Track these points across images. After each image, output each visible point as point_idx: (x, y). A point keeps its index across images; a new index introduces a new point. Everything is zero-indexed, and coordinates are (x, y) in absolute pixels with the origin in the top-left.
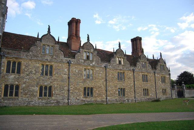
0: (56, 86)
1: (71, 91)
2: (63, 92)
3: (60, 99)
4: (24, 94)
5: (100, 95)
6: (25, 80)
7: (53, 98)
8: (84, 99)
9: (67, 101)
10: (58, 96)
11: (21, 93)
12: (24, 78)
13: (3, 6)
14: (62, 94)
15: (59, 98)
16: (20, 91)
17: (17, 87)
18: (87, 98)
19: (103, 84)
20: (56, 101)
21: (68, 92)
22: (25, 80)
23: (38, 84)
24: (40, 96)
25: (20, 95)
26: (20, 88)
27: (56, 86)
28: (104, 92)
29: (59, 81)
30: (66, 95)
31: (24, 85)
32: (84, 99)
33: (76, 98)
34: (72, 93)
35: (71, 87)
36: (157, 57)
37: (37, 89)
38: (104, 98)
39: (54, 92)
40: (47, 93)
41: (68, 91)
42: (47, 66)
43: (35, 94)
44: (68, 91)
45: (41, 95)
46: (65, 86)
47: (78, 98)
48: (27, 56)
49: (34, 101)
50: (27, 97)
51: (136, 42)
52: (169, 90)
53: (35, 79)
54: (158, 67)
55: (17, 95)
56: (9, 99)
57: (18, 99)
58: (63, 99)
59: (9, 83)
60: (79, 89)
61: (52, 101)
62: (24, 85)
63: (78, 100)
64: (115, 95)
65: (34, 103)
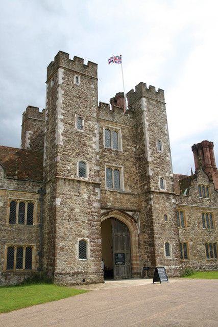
4: (193, 255)
13: (167, 137)
16: (189, 251)
23: (203, 241)
25: (190, 256)
31: (191, 243)
37: (203, 247)
42: (207, 214)
48: (188, 201)
62: (191, 243)
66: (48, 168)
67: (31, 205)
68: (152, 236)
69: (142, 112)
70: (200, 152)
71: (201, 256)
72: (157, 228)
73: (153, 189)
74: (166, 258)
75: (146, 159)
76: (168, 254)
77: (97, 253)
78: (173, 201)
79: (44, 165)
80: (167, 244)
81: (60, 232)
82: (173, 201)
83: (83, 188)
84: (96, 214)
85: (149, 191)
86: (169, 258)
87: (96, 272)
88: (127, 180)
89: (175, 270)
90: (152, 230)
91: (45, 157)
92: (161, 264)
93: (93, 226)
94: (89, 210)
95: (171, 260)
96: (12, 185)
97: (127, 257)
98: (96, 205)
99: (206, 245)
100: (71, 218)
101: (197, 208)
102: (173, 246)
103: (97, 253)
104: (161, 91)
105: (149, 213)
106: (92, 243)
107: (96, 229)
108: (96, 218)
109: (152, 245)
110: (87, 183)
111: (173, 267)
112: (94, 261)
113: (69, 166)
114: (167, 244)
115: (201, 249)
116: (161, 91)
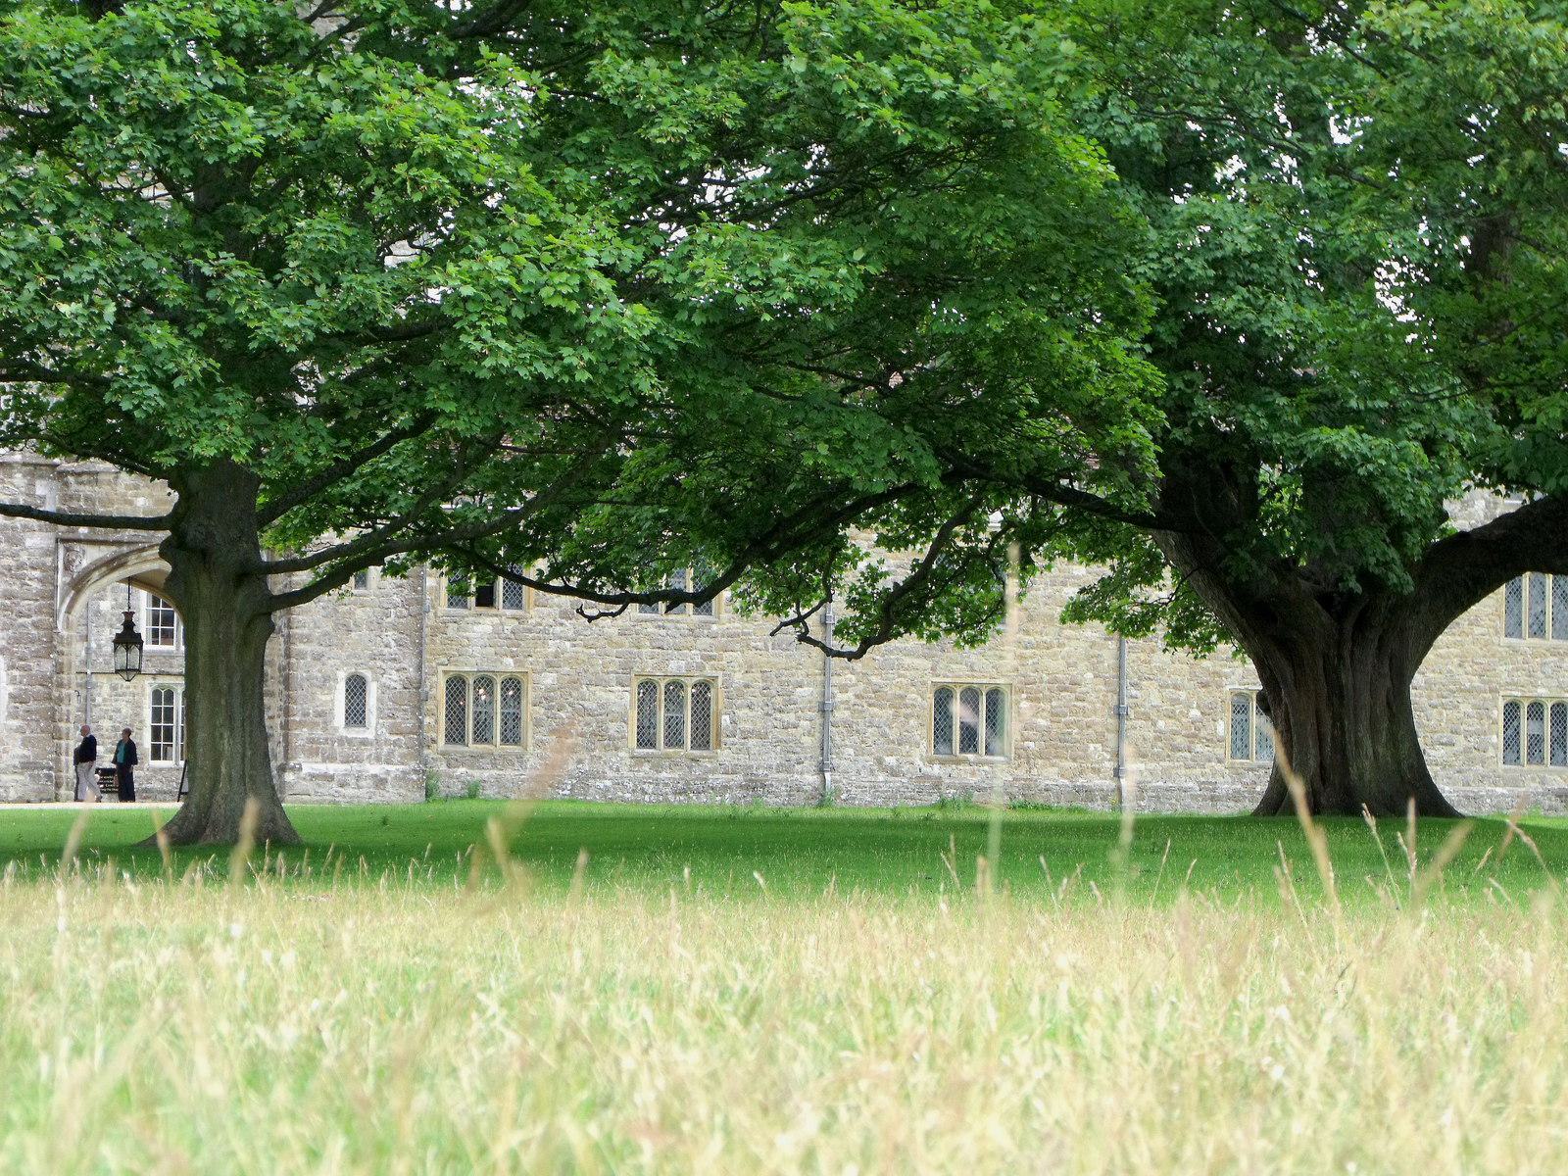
0: (738, 678)
1: (840, 715)
2: (790, 718)
3: (770, 767)
4: (552, 732)
5: (1057, 745)
6: (552, 646)
7: (724, 755)
8: (936, 770)
9: (811, 779)
10: (751, 742)
11: (538, 723)
12: (544, 631)
14: (782, 735)
15: (764, 759)
16: (530, 711)
17: (514, 685)
18: (958, 762)
19: (1094, 662)
20: (739, 778)
21: (819, 721)
22: (552, 646)
23: (627, 668)
24: (641, 743)
26: (530, 695)
27: (738, 678)
28: (1104, 719)
29: (760, 645)
30: (807, 740)
31: (549, 679)
32: (936, 770)
33: (880, 761)
34: (848, 725)
35: (844, 689)
37: (624, 699)
38: (1096, 771)
39: (726, 720)
40: (680, 722)
41: (824, 710)
43: (613, 728)
44: (824, 710)
45: (646, 739)
46: (800, 676)
47: (890, 760)
49: (610, 774)
50: (573, 750)
53: (609, 639)
55: (512, 735)
56: (474, 760)
57: (520, 757)
58: (786, 768)
59: (468, 667)
60: (898, 702)
61: (719, 779)
62: (549, 679)
63: (894, 772)
64: (1199, 748)
65: (608, 783)
71: (599, 736)
74: (343, 732)
76: (356, 714)
77: (33, 705)
80: (356, 687)
84: (37, 574)
86: (356, 733)
87: (26, 766)
89: (380, 782)
92: (312, 753)
93: (20, 614)
94: (9, 562)
95: (364, 742)
97: (437, 721)
99: (648, 687)
102: (384, 688)
103: (33, 705)
106: (16, 673)
107: (35, 625)
108: (35, 585)
111: (376, 769)
112: (20, 730)
114: (356, 687)
115: (602, 706)
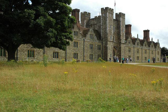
36: (155, 41)
51: (146, 33)
52: (160, 59)
54: (157, 47)
66: (103, 37)
67: (100, 46)
68: (120, 53)
69: (120, 21)
70: (127, 28)
72: (122, 52)
73: (121, 42)
75: (120, 35)
78: (125, 45)
79: (101, 36)
81: (108, 52)
82: (125, 45)
83: (111, 43)
85: (120, 43)
88: (115, 39)
90: (121, 52)
91: (102, 34)
96: (98, 41)
98: (113, 46)
100: (110, 49)
101: (128, 47)
104: (124, 14)
105: (120, 48)
109: (120, 55)
110: (112, 42)
113: (109, 38)
116: (124, 14)
